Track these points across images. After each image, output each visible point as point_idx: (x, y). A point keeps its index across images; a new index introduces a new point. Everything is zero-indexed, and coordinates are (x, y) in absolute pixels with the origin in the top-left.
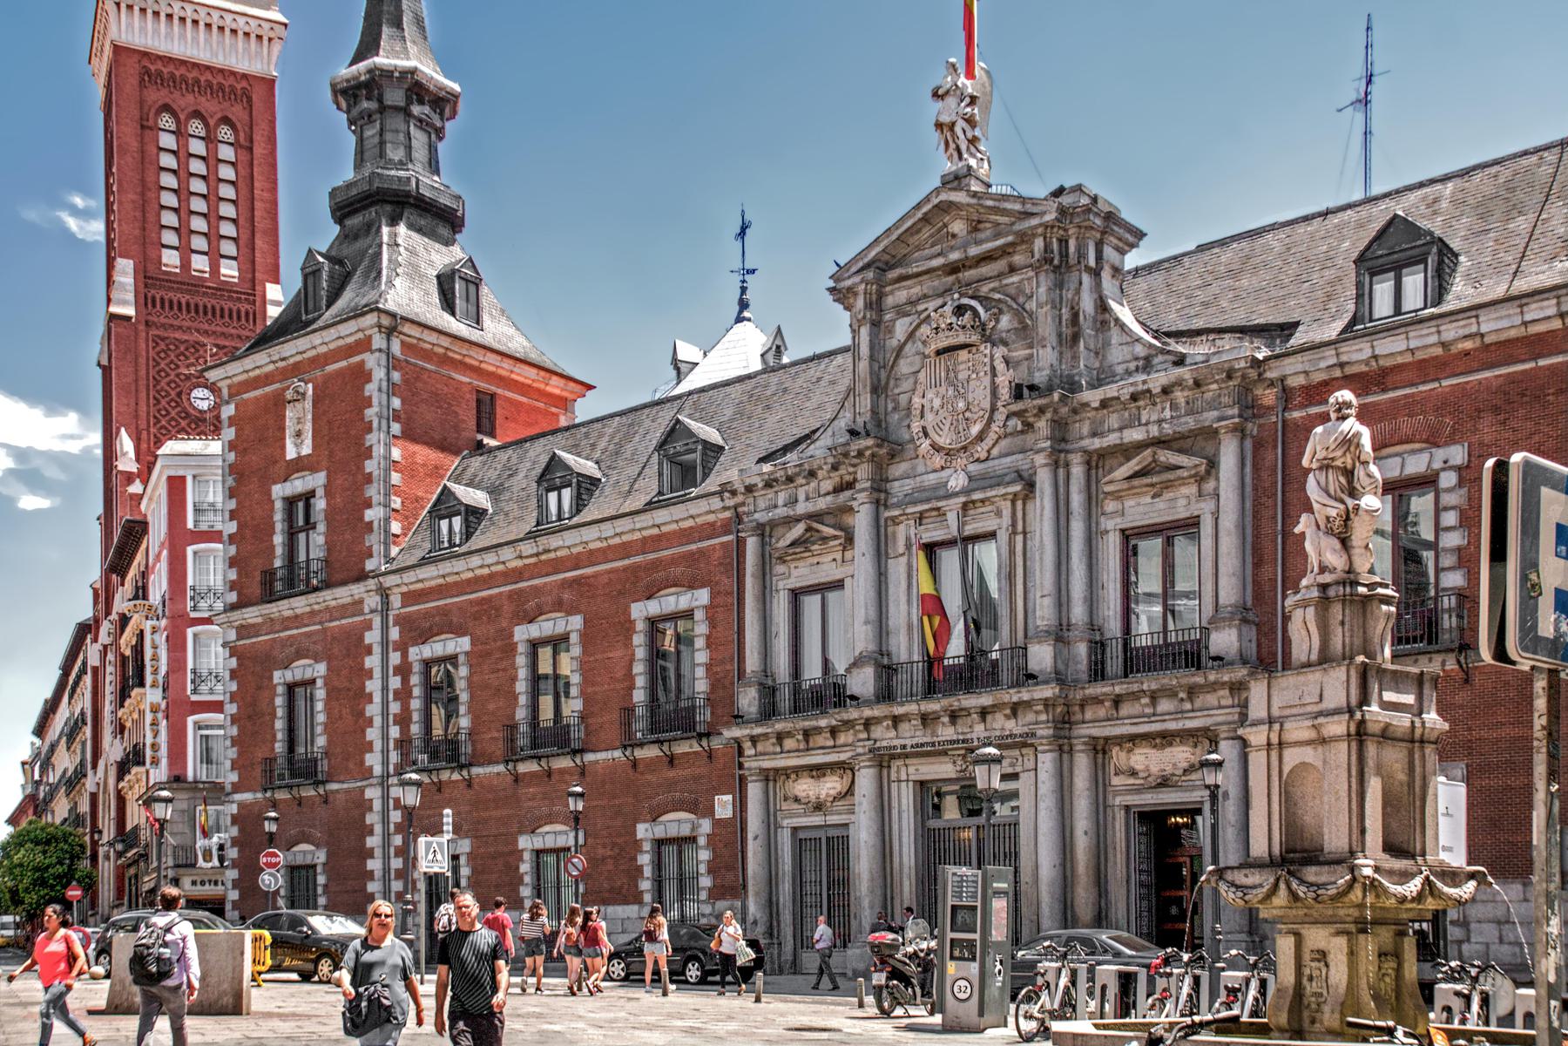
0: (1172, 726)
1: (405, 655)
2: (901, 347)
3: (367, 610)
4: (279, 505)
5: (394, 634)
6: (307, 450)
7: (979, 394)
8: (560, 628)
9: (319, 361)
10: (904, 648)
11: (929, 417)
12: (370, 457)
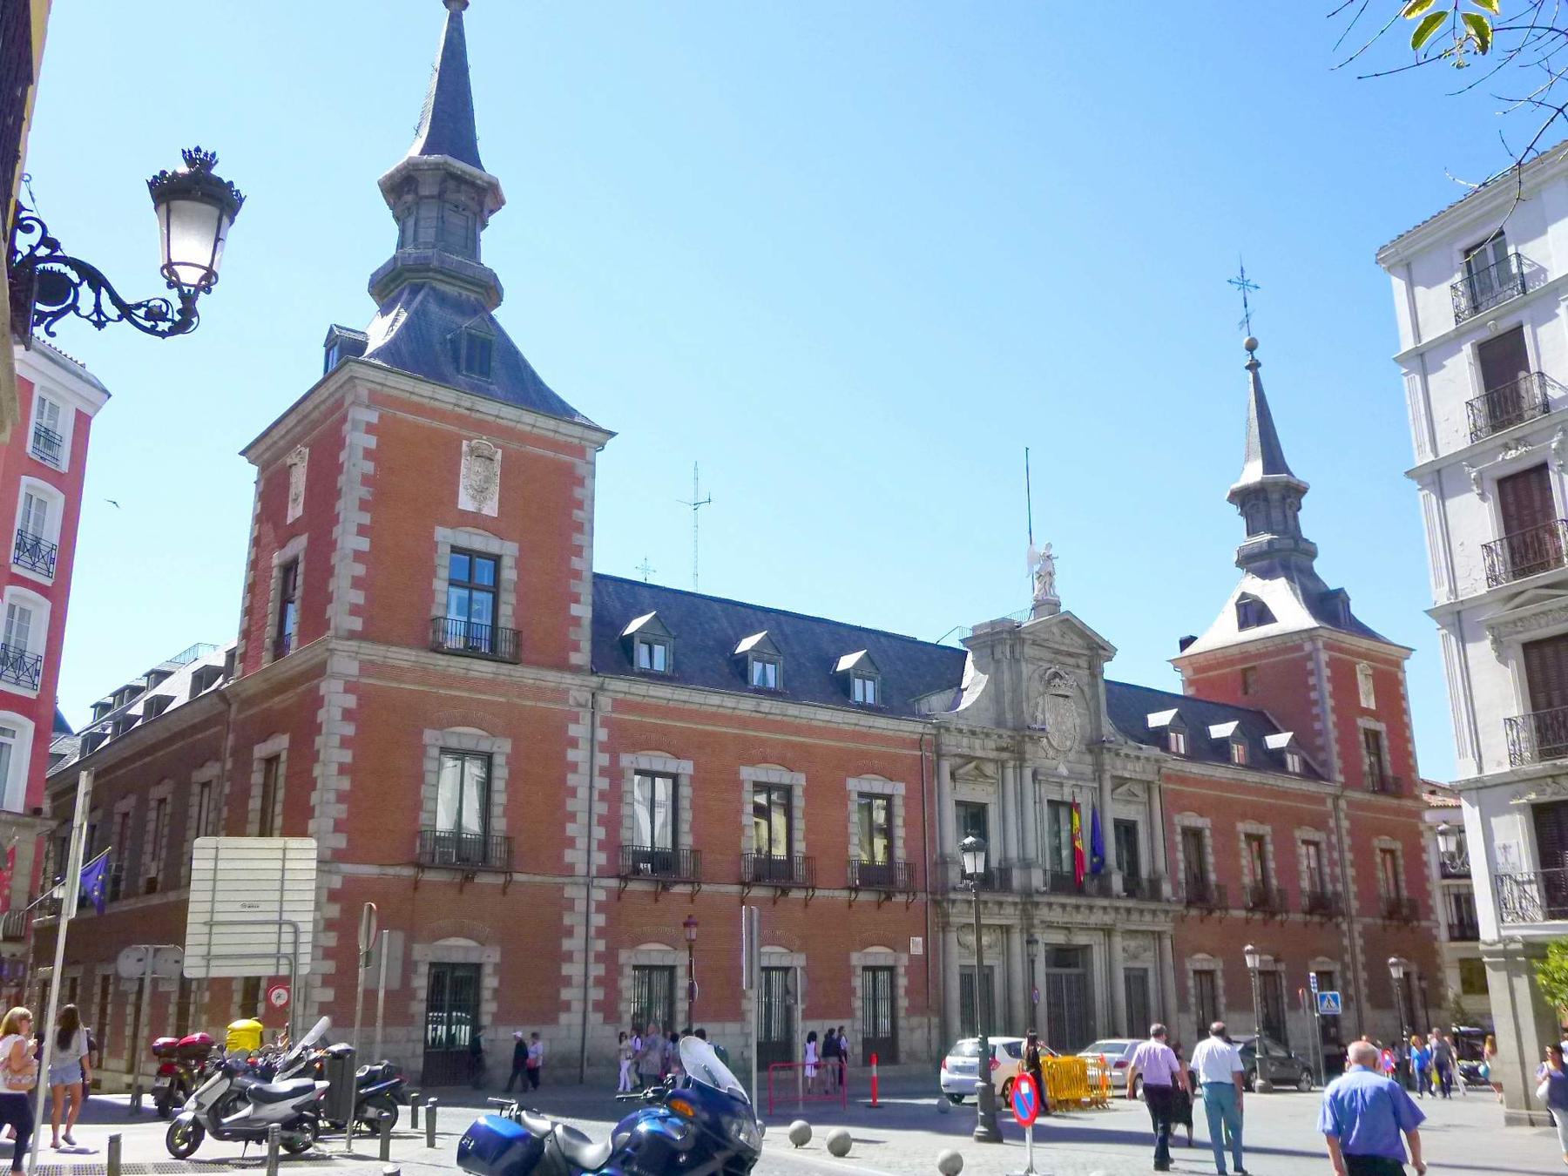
1: (615, 760)
3: (571, 701)
5: (602, 734)
6: (491, 509)
9: (523, 438)
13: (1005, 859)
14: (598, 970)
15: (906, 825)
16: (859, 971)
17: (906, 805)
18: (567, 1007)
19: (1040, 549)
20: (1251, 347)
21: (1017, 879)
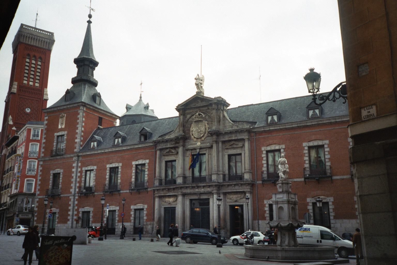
0: (238, 190)
1: (81, 169)
2: (188, 119)
4: (56, 137)
5: (80, 164)
7: (203, 129)
8: (117, 165)
10: (188, 173)
11: (193, 132)
12: (78, 129)
14: (75, 213)
16: (133, 210)
18: (69, 220)
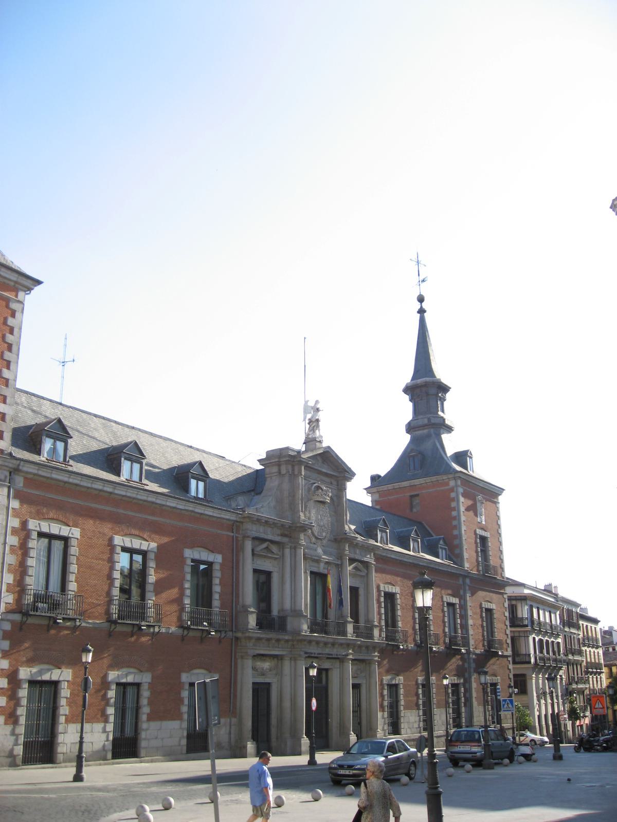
13: (281, 610)
15: (220, 584)
16: (187, 687)
17: (222, 570)
19: (311, 404)
20: (421, 299)
21: (291, 624)
